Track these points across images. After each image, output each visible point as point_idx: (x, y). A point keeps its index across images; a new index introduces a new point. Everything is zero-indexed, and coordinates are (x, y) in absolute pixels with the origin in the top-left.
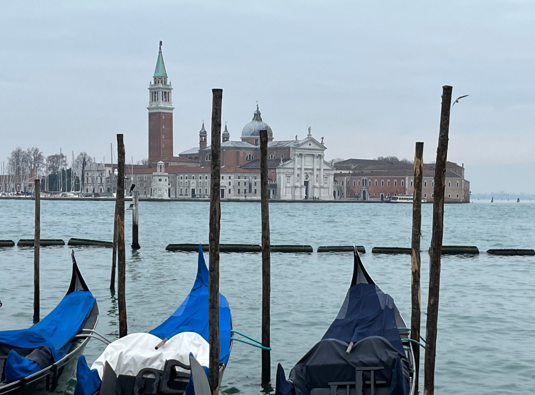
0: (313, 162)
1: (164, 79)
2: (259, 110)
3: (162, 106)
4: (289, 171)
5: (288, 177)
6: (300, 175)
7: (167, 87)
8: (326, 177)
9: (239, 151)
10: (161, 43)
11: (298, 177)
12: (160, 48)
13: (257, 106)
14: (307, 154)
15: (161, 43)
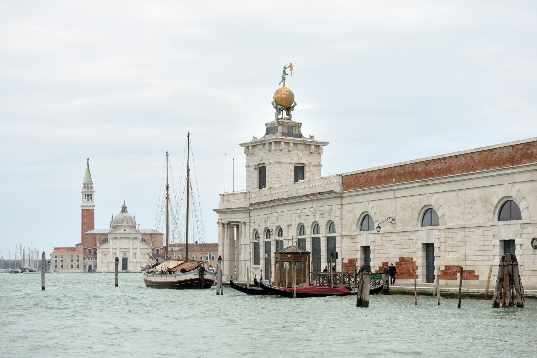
0: (130, 243)
1: (88, 185)
2: (125, 204)
3: (84, 205)
4: (106, 251)
5: (104, 255)
6: (116, 253)
7: (90, 190)
8: (143, 254)
9: (95, 236)
10: (88, 159)
11: (115, 255)
12: (88, 163)
13: (124, 201)
14: (121, 237)
15: (88, 159)
